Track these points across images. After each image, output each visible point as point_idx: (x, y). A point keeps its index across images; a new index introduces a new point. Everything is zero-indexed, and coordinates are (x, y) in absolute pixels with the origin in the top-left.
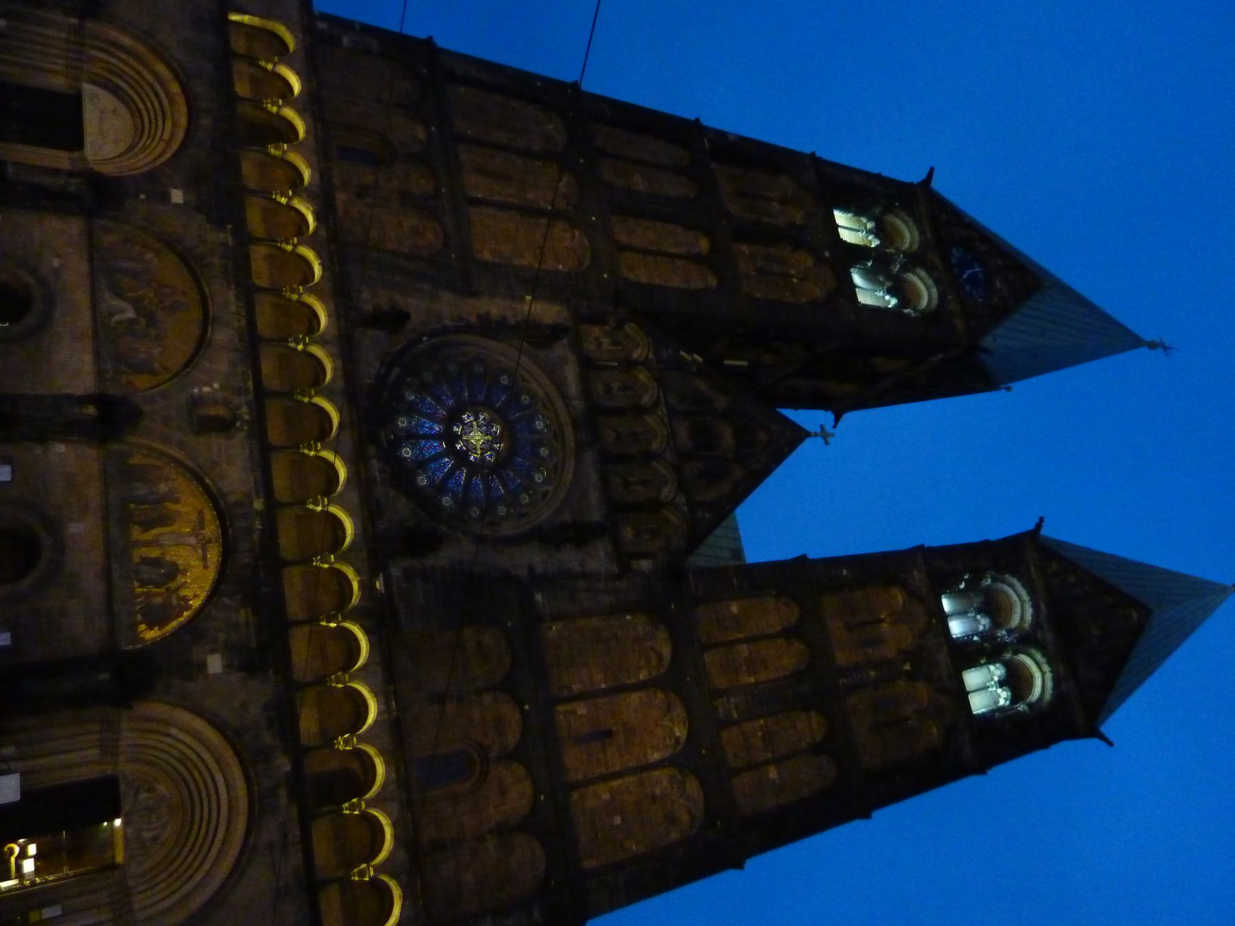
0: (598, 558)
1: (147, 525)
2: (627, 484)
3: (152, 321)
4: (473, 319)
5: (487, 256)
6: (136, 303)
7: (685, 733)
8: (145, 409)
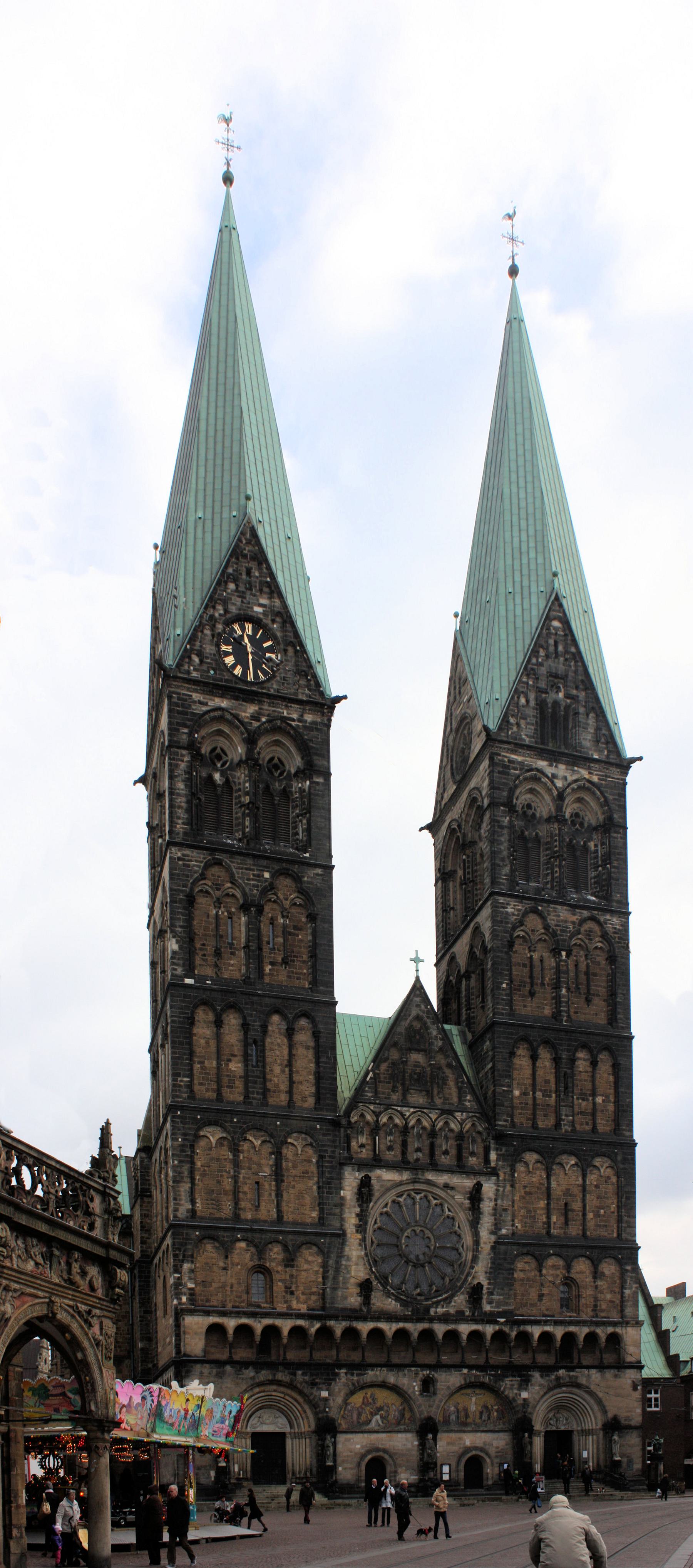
0: (489, 1188)
1: (467, 1416)
2: (446, 1152)
3: (380, 1409)
4: (359, 1236)
5: (315, 1214)
6: (373, 1414)
7: (573, 1158)
8: (426, 1414)
